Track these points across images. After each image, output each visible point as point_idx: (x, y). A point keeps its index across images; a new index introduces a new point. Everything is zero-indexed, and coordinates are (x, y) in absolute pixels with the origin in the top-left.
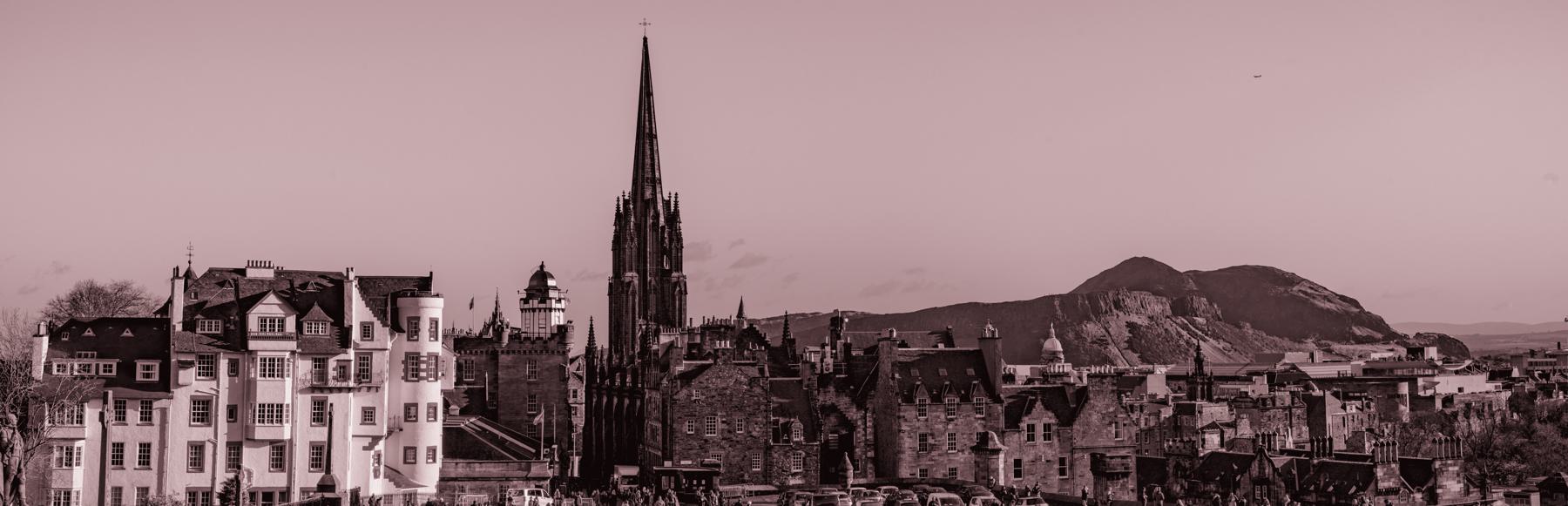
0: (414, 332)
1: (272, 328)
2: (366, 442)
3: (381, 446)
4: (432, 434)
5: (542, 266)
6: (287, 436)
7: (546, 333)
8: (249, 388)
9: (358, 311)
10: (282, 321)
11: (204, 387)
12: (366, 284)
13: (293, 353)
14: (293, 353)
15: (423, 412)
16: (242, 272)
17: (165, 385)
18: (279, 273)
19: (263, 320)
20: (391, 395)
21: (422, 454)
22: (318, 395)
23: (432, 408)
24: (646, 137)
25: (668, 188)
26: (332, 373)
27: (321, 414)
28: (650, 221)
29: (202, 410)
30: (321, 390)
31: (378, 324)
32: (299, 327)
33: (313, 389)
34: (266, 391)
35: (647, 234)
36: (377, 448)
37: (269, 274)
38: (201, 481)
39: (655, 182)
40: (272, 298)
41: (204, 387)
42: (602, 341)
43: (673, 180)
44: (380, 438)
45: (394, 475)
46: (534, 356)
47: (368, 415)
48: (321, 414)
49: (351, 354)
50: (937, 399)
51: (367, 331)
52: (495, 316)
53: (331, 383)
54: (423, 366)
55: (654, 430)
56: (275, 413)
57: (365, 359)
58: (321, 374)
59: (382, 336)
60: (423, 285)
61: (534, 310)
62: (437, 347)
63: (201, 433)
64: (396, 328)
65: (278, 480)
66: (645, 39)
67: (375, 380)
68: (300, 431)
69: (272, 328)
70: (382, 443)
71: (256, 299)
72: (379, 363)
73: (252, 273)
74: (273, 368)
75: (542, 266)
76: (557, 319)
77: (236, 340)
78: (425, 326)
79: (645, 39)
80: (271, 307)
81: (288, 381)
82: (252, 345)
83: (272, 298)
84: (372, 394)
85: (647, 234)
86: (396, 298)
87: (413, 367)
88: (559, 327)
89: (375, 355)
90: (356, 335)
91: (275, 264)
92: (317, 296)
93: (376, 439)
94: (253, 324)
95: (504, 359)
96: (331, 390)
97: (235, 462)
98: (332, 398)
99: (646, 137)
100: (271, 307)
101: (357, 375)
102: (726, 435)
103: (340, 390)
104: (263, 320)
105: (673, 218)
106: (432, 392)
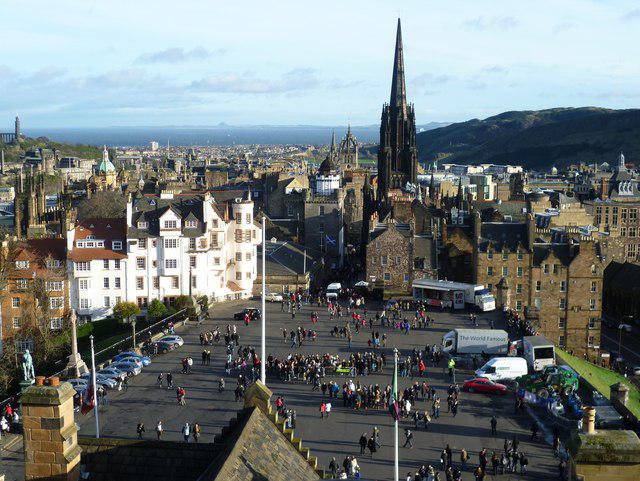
1: (171, 225)
3: (223, 274)
4: (249, 266)
8: (160, 254)
11: (142, 253)
15: (244, 257)
17: (124, 252)
21: (244, 276)
24: (398, 73)
27: (193, 263)
28: (398, 119)
29: (141, 262)
32: (183, 223)
33: (189, 252)
34: (169, 254)
38: (143, 293)
39: (403, 97)
41: (142, 253)
43: (413, 97)
47: (217, 261)
48: (193, 263)
49: (207, 236)
50: (499, 250)
51: (215, 222)
52: (348, 136)
56: (172, 264)
57: (215, 236)
58: (193, 246)
63: (142, 273)
65: (176, 293)
68: (183, 270)
69: (171, 225)
72: (221, 237)
74: (172, 244)
77: (154, 230)
78: (244, 217)
80: (170, 216)
82: (162, 234)
84: (218, 251)
87: (238, 236)
88: (335, 190)
90: (210, 226)
93: (221, 271)
94: (162, 225)
97: (157, 285)
99: (398, 73)
100: (170, 216)
105: (411, 116)
106: (248, 248)
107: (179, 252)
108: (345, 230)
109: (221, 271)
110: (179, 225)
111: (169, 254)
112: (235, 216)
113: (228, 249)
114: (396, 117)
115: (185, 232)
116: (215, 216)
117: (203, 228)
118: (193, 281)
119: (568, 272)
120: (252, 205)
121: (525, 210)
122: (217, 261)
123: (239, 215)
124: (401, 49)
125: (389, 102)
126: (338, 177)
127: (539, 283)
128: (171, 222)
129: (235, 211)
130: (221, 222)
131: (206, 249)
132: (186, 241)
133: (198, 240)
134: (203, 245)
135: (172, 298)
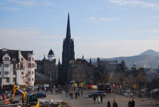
0: (30, 60)
2: (22, 77)
3: (25, 78)
4: (33, 76)
5: (51, 50)
6: (9, 77)
7: (51, 60)
9: (20, 56)
10: (8, 58)
12: (23, 53)
13: (10, 63)
14: (10, 63)
15: (31, 73)
16: (2, 50)
18: (8, 50)
19: (5, 58)
20: (26, 71)
21: (31, 80)
22: (14, 70)
23: (33, 72)
25: (72, 37)
26: (16, 66)
27: (15, 73)
30: (15, 69)
31: (24, 59)
34: (6, 69)
35: (68, 45)
36: (24, 78)
37: (6, 50)
40: (7, 54)
42: (61, 62)
44: (24, 77)
45: (26, 83)
46: (50, 64)
47: (22, 73)
48: (15, 73)
49: (20, 63)
51: (22, 59)
53: (16, 68)
54: (31, 65)
55: (69, 76)
56: (7, 73)
57: (22, 64)
60: (31, 52)
61: (50, 57)
62: (34, 62)
64: (27, 59)
65: (8, 84)
68: (11, 76)
69: (7, 59)
70: (25, 78)
71: (4, 54)
72: (24, 65)
73: (3, 50)
74: (7, 66)
75: (51, 50)
76: (53, 58)
78: (32, 59)
80: (7, 56)
81: (9, 68)
82: (3, 62)
83: (7, 54)
85: (68, 45)
86: (26, 54)
87: (30, 66)
89: (23, 63)
90: (20, 60)
91: (7, 49)
92: (14, 54)
93: (24, 77)
94: (3, 58)
95: (45, 65)
96: (16, 69)
98: (17, 71)
100: (7, 56)
102: (80, 77)
103: (18, 69)
104: (5, 58)
106: (33, 69)
107: (10, 69)
109: (24, 77)
110: (10, 59)
111: (6, 69)
112: (28, 59)
113: (26, 71)
115: (12, 62)
116: (22, 57)
117: (18, 60)
118: (15, 79)
119: (136, 78)
122: (22, 73)
123: (30, 58)
124: (69, 22)
127: (127, 82)
128: (7, 58)
129: (28, 57)
130: (24, 60)
132: (12, 66)
133: (16, 65)
134: (18, 65)
135: (6, 86)
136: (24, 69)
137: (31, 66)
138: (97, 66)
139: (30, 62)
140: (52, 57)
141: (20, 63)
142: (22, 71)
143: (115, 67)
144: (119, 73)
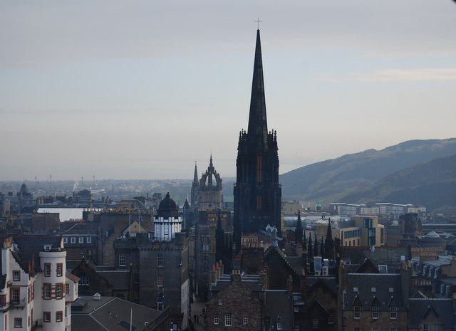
15: (53, 317)
23: (59, 315)
25: (271, 126)
31: (22, 271)
47: (18, 322)
49: (6, 291)
51: (16, 273)
57: (15, 291)
59: (28, 280)
61: (161, 223)
66: (258, 31)
67: (22, 304)
78: (54, 268)
79: (258, 31)
87: (49, 292)
88: (176, 234)
90: (9, 278)
95: (143, 254)
101: (11, 302)
108: (191, 284)
112: (43, 267)
114: (257, 147)
116: (17, 267)
120: (65, 253)
121: (403, 258)
123: (48, 266)
125: (246, 129)
126: (180, 219)
129: (43, 261)
130: (24, 275)
131: (5, 308)
136: (23, 308)
137: (50, 293)
138: (327, 271)
139: (48, 280)
140: (171, 223)
141: (6, 291)
142: (18, 314)
143: (374, 290)
144: (385, 314)
